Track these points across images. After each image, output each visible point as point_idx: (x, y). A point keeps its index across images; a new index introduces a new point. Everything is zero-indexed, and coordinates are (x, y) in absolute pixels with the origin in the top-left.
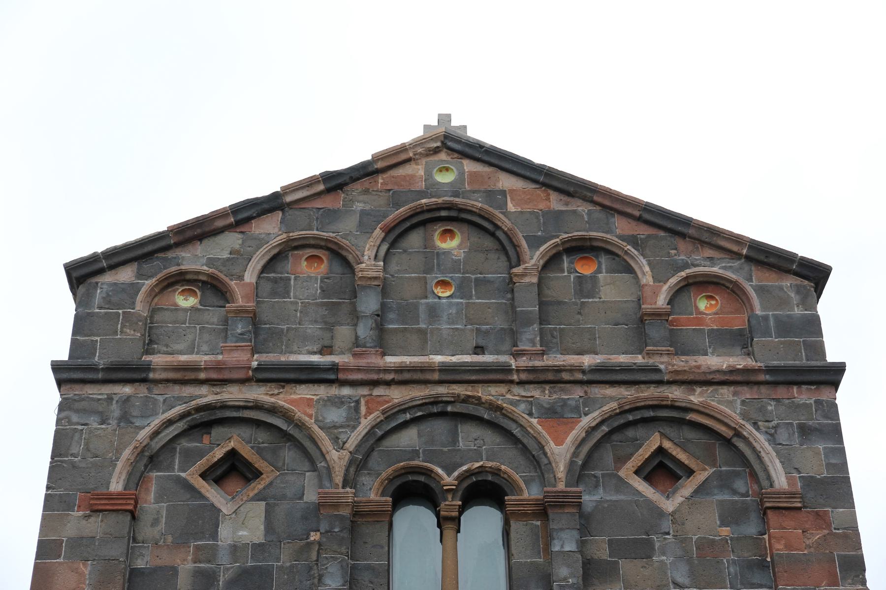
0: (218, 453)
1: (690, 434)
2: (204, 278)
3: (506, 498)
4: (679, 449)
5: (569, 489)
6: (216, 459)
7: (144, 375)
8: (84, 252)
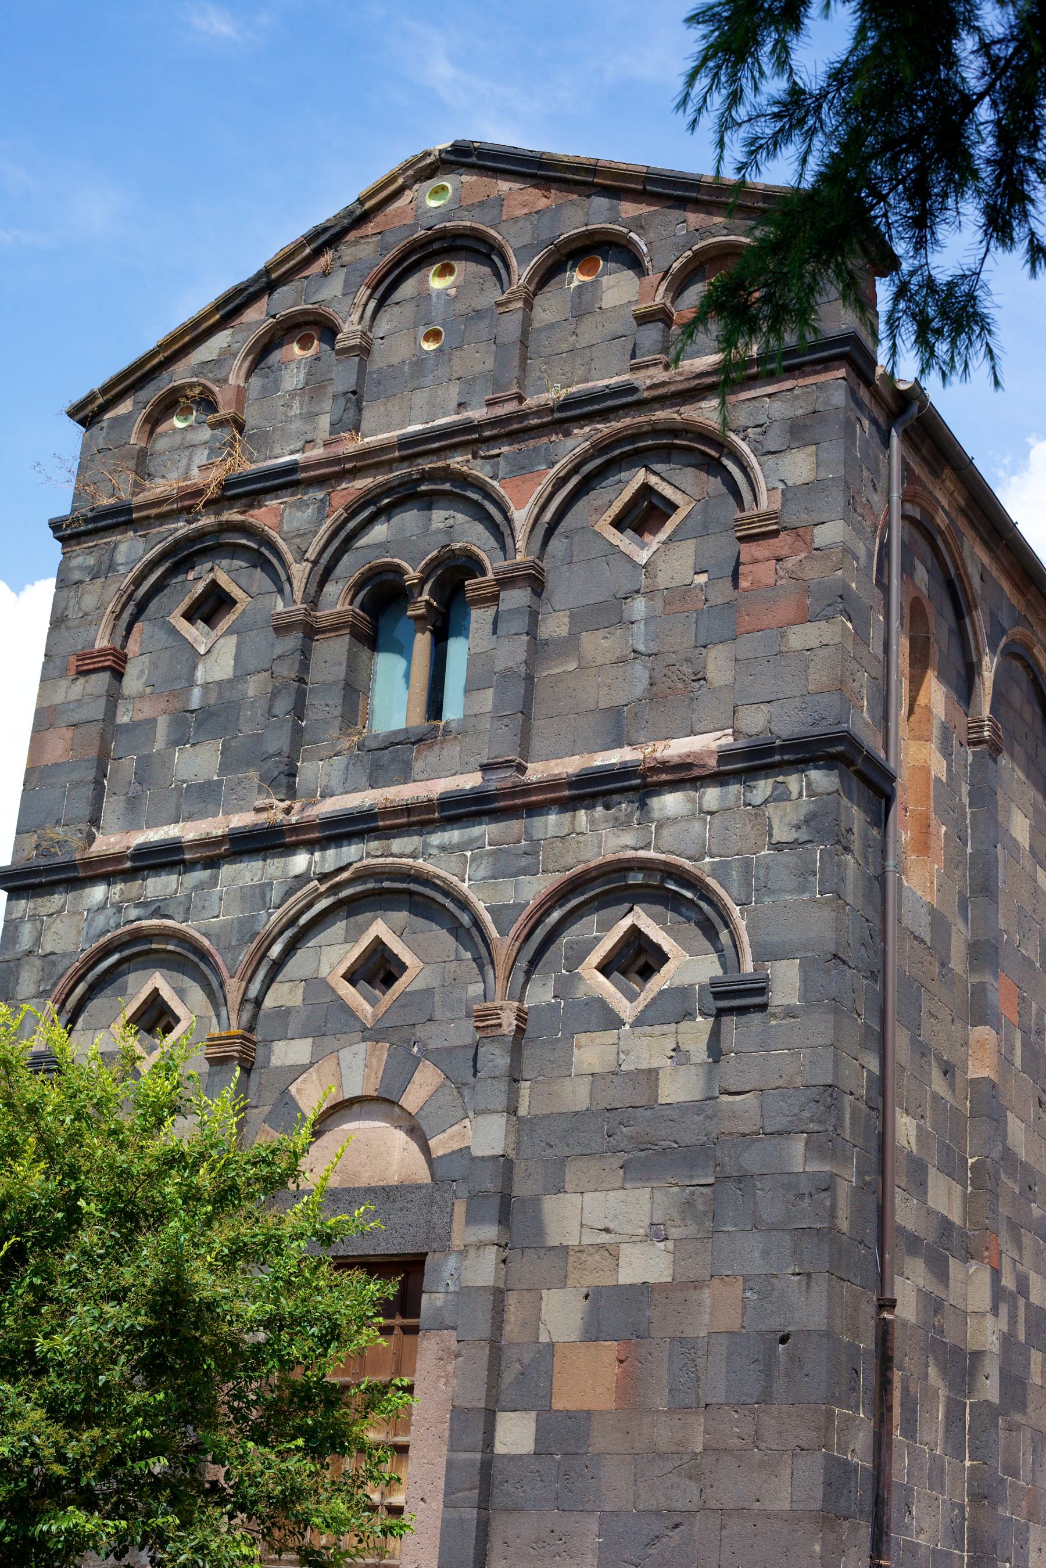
0: (200, 587)
8: (79, 395)
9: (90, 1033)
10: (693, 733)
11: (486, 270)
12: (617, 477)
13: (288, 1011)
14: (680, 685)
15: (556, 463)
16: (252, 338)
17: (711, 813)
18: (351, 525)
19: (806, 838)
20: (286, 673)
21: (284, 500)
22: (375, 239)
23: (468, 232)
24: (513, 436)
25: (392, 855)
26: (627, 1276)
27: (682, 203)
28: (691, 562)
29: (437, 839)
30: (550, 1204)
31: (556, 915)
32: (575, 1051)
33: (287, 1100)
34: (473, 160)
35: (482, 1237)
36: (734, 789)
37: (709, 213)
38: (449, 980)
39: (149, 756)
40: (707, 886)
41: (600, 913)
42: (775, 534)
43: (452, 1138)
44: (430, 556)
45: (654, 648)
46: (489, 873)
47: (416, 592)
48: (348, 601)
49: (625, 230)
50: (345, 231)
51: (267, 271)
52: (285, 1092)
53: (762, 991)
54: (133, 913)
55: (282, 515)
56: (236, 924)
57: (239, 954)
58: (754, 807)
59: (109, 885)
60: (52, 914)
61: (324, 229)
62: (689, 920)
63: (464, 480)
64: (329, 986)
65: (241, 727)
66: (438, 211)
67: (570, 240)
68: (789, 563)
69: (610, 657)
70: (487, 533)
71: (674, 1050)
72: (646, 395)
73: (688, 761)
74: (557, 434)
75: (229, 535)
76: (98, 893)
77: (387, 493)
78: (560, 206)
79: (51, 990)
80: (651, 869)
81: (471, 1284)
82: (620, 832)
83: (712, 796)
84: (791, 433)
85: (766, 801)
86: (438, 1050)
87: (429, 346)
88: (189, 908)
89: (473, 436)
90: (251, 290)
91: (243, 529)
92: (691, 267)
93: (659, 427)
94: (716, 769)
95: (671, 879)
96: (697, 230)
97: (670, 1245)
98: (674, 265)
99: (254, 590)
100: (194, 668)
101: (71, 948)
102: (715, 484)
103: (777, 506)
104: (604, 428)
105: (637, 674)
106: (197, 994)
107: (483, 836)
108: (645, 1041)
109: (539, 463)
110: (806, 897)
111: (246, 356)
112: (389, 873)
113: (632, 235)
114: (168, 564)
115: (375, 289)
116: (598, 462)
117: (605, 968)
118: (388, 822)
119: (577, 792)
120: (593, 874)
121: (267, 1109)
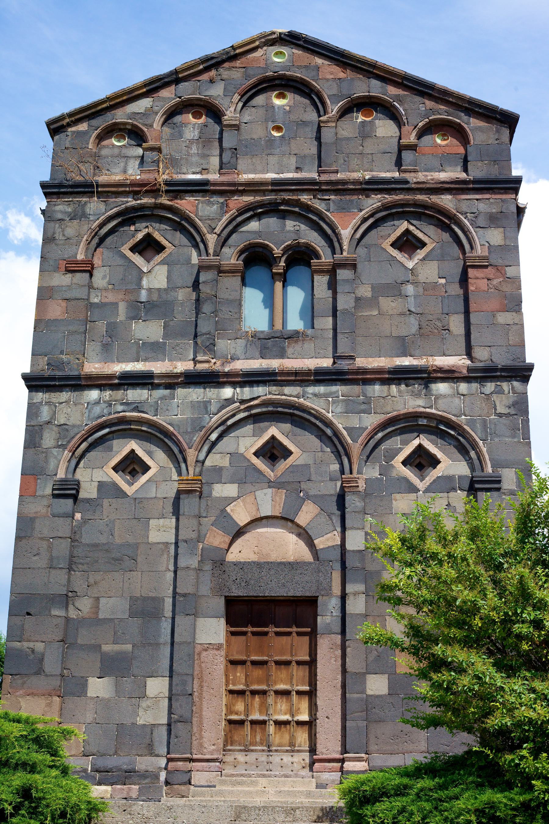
0: (140, 236)
2: (129, 127)
3: (312, 261)
4: (418, 231)
5: (349, 256)
6: (138, 240)
9: (89, 470)
10: (444, 355)
11: (307, 102)
12: (392, 223)
13: (221, 469)
14: (436, 331)
15: (363, 210)
16: (167, 106)
17: (463, 395)
18: (240, 219)
19: (514, 412)
20: (209, 291)
21: (198, 198)
22: (240, 70)
23: (299, 80)
24: (337, 192)
25: (285, 395)
27: (422, 94)
28: (436, 272)
29: (311, 390)
31: (380, 435)
32: (394, 502)
33: (225, 514)
34: (301, 43)
35: (356, 590)
36: (475, 386)
37: (437, 103)
38: (318, 461)
39: (115, 323)
40: (464, 429)
41: (402, 436)
42: (486, 267)
43: (328, 540)
44: (287, 244)
45: (419, 310)
46: (344, 411)
47: (278, 260)
48: (236, 259)
49: (391, 100)
50: (223, 61)
51: (176, 72)
52: (224, 511)
53: (499, 482)
54: (120, 408)
55: (197, 207)
56: (189, 420)
57: (194, 437)
58: (485, 395)
59: (101, 391)
60: (62, 403)
61: (212, 58)
62: (450, 444)
63: (308, 208)
64: (245, 458)
65: (176, 315)
66: (280, 64)
67: (359, 98)
68: (495, 282)
69: (395, 311)
70: (320, 238)
71: (447, 505)
72: (413, 186)
73: (453, 369)
74: (362, 195)
75: (160, 211)
76: (94, 394)
77: (261, 206)
78: (352, 79)
79: (66, 445)
80: (431, 418)
81: (352, 612)
82: (416, 399)
83: (463, 387)
84: (490, 220)
85: (492, 393)
86: (315, 496)
87: (276, 134)
88: (157, 409)
89: (316, 187)
90: (166, 80)
91: (170, 209)
92: (426, 127)
93: (418, 203)
94: (467, 375)
95: (442, 424)
96: (431, 109)
98: (420, 124)
99: (176, 243)
100: (141, 279)
101: (79, 423)
102: (446, 236)
103: (486, 254)
104: (389, 198)
105: (412, 322)
106: (160, 455)
107: (338, 391)
109: (353, 208)
110: (516, 440)
111: (163, 115)
112: (281, 404)
113: (395, 103)
114: (120, 220)
115: (242, 97)
116: (384, 213)
117: (404, 463)
118: (283, 378)
119: (393, 376)
120: (401, 417)
121: (213, 518)
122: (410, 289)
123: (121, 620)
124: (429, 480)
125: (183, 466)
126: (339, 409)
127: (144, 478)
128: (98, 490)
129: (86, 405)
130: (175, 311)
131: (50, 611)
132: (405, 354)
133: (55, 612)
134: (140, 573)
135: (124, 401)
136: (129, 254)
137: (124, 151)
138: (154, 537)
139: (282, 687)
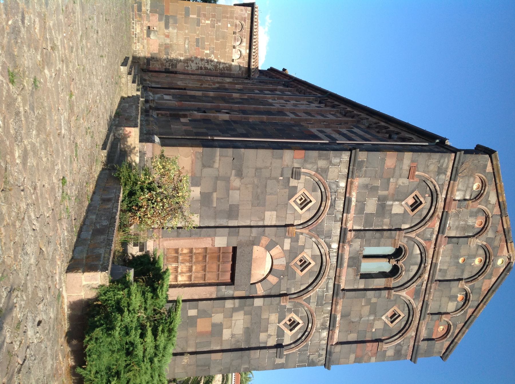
0: (422, 199)
1: (403, 323)
7: (452, 179)
10: (339, 332)
18: (421, 247)
19: (309, 361)
25: (329, 271)
26: (225, 331)
30: (242, 312)
39: (378, 190)
44: (404, 266)
45: (360, 322)
52: (277, 244)
54: (333, 197)
55: (431, 228)
76: (343, 184)
97: (230, 339)
108: (274, 329)
110: (297, 362)
121: (274, 240)
122: (372, 318)
123: (228, 201)
124: (283, 328)
125: (301, 227)
126: (320, 294)
127: (298, 209)
128: (293, 186)
129: (338, 181)
130: (379, 218)
131: (234, 169)
132: (342, 316)
133: (234, 172)
134: (250, 208)
135: (337, 199)
136: (413, 195)
137: (469, 189)
138: (268, 214)
139: (194, 268)
